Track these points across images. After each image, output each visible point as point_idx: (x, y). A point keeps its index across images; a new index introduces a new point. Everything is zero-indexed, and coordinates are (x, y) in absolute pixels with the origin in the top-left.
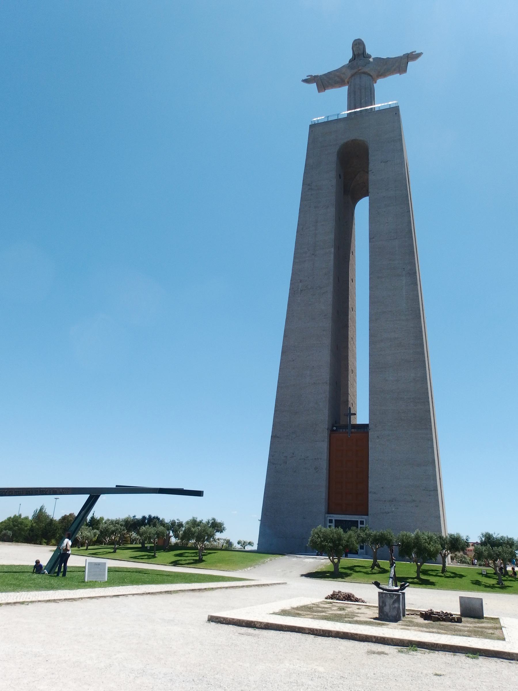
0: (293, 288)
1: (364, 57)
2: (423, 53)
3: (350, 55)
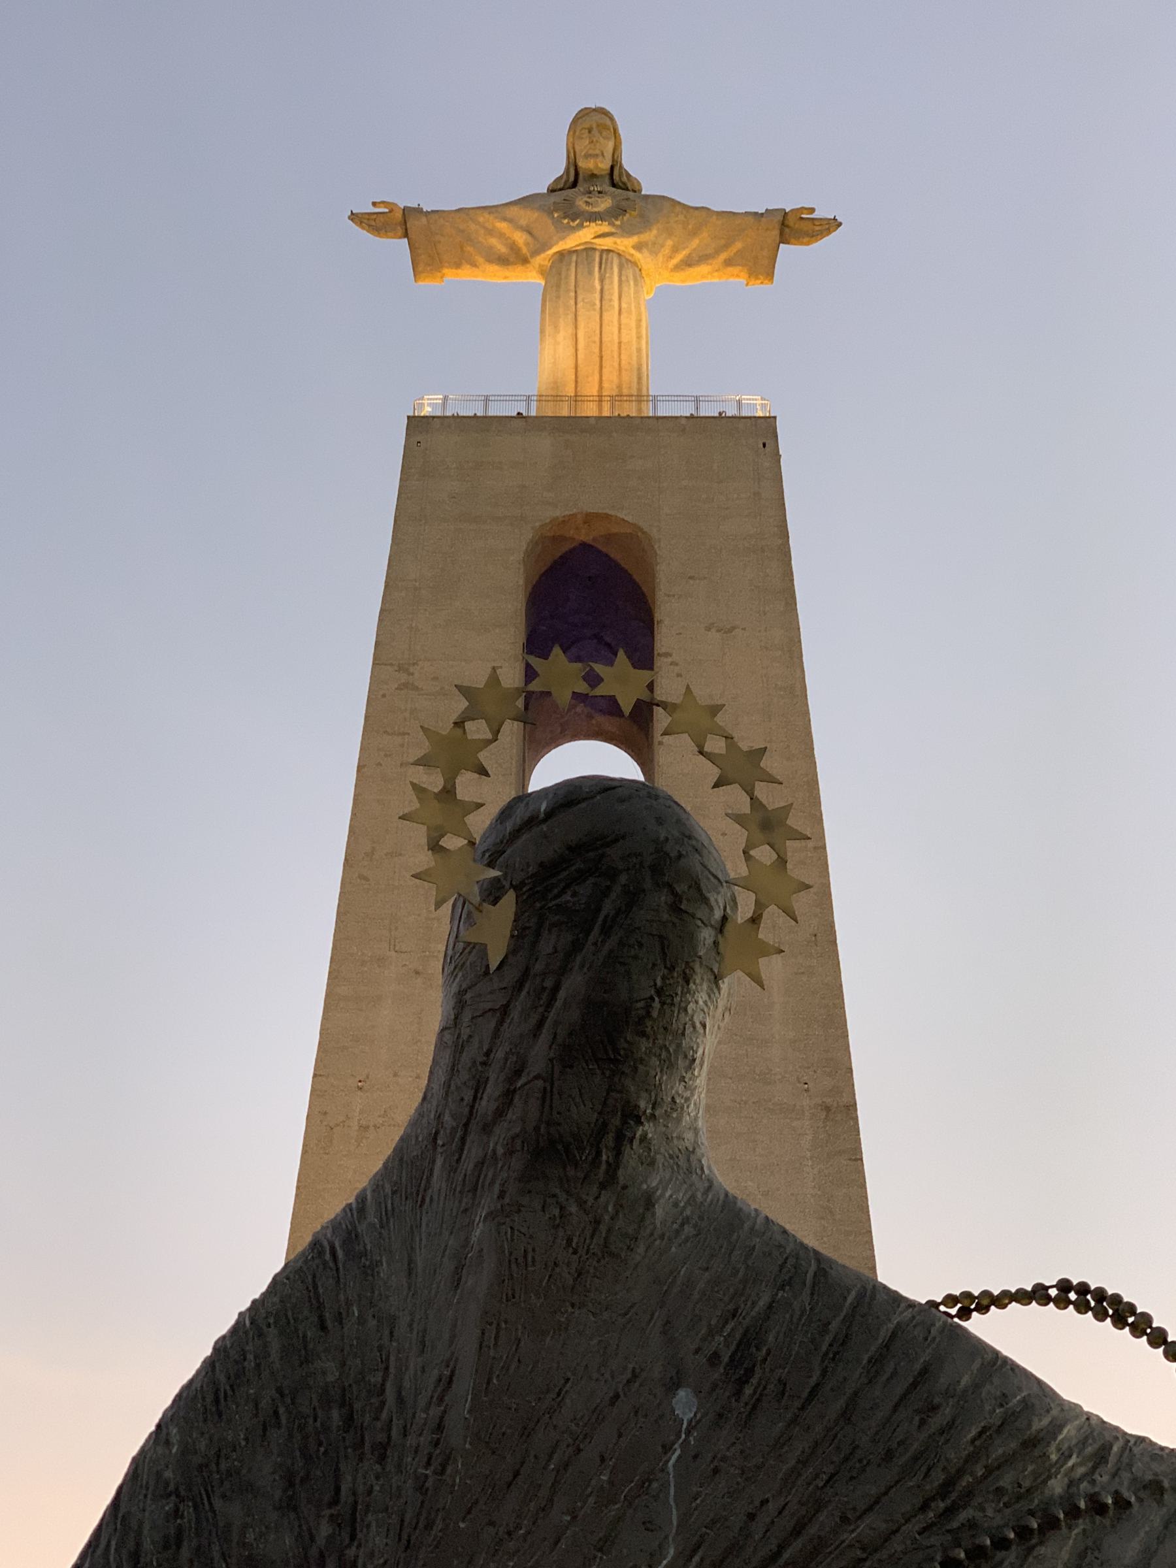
0: (325, 1113)
1: (614, 185)
2: (840, 224)
3: (557, 168)
